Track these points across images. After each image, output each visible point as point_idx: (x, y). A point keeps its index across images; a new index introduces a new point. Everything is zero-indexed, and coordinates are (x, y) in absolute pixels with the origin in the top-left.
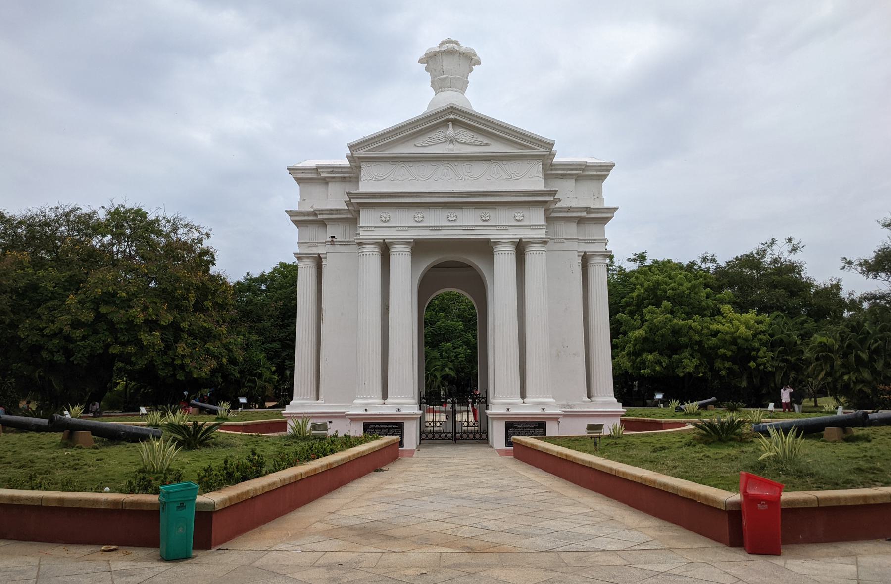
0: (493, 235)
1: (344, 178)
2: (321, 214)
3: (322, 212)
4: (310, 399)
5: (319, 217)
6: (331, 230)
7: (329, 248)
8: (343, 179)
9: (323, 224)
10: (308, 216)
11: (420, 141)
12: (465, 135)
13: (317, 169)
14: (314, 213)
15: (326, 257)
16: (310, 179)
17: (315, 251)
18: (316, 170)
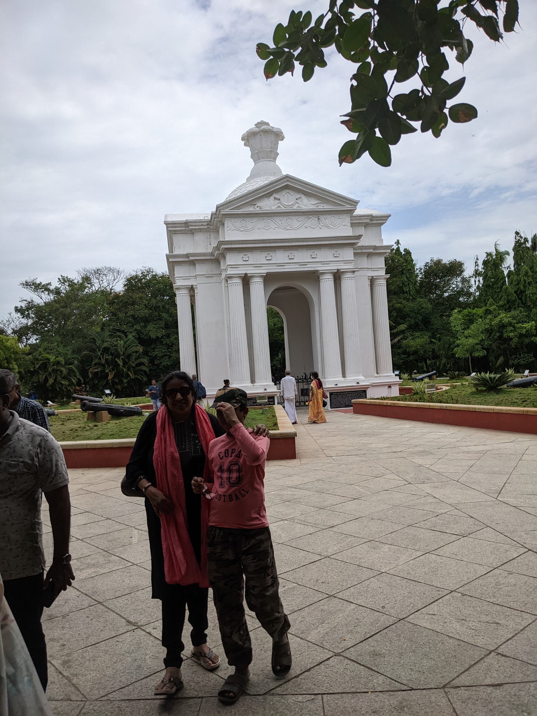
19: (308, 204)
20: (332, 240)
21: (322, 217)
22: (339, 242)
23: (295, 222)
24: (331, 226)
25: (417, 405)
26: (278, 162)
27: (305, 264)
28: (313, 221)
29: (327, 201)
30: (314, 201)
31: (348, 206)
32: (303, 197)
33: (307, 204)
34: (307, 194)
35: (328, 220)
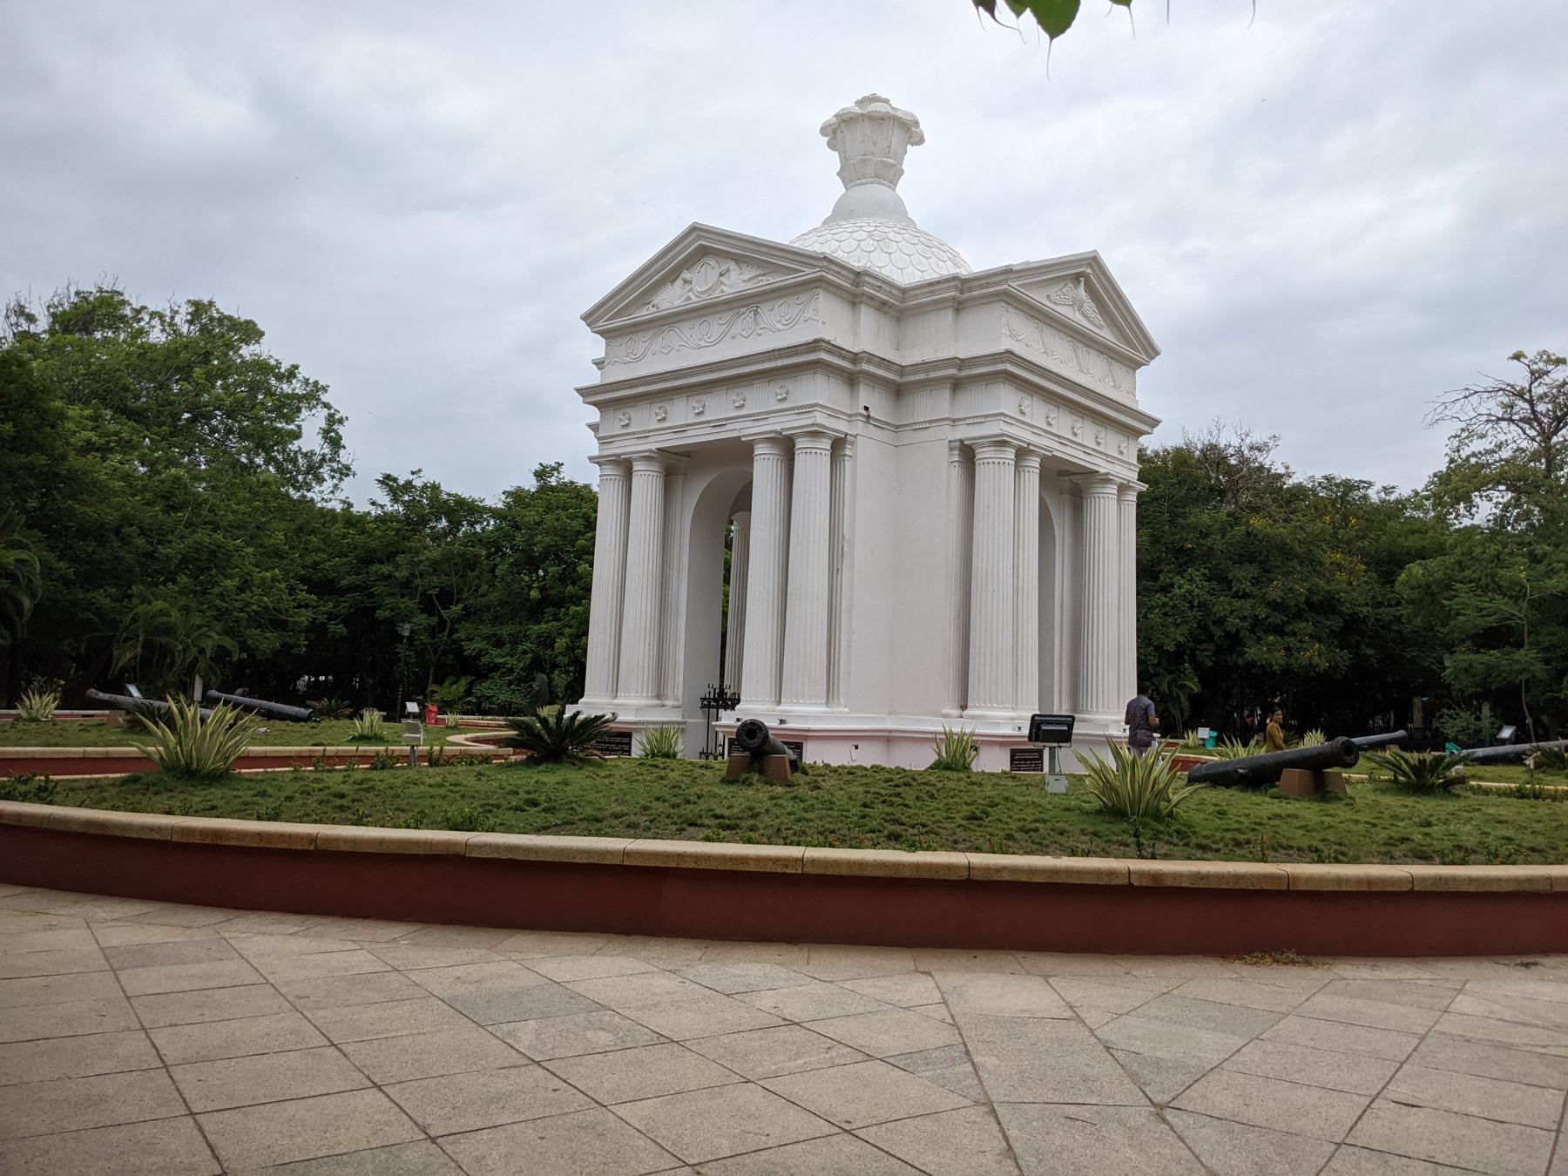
0: (1103, 467)
1: (884, 303)
2: (869, 362)
3: (871, 358)
4: (817, 704)
5: (865, 367)
6: (866, 396)
7: (859, 427)
8: (882, 307)
9: (851, 380)
10: (844, 358)
11: (1052, 291)
12: (1089, 306)
13: (858, 274)
14: (855, 358)
15: (852, 443)
16: (838, 287)
17: (841, 426)
18: (858, 276)
19: (738, 281)
20: (763, 361)
21: (764, 310)
22: (779, 363)
23: (715, 326)
24: (779, 326)
25: (1054, 871)
26: (902, 188)
27: (719, 424)
28: (746, 321)
29: (775, 269)
30: (749, 273)
31: (807, 271)
32: (732, 265)
33: (738, 281)
34: (738, 259)
35: (772, 315)
